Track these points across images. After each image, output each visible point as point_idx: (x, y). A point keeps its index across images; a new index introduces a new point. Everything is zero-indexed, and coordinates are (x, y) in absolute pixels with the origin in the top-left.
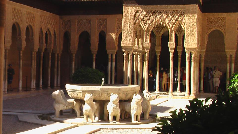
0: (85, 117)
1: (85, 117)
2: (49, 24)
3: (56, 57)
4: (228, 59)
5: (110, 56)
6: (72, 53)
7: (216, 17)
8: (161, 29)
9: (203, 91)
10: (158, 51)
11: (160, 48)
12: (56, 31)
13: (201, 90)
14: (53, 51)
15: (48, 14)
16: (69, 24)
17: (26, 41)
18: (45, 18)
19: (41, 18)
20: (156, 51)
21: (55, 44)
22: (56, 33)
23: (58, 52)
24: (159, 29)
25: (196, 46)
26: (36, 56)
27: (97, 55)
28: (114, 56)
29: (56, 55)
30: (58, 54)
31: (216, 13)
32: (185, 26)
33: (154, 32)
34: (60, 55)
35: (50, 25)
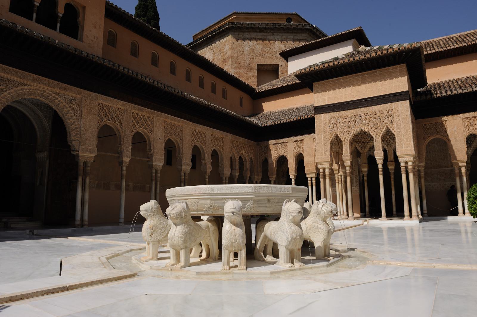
2: (243, 150)
4: (457, 172)
5: (309, 179)
6: (270, 179)
7: (434, 122)
8: (366, 144)
9: (426, 215)
10: (365, 169)
11: (367, 165)
12: (253, 158)
13: (425, 213)
15: (241, 139)
16: (266, 150)
17: (212, 165)
18: (237, 143)
19: (233, 143)
24: (363, 144)
25: (427, 70)
28: (314, 179)
31: (433, 118)
32: (395, 130)
33: (358, 148)
35: (245, 150)
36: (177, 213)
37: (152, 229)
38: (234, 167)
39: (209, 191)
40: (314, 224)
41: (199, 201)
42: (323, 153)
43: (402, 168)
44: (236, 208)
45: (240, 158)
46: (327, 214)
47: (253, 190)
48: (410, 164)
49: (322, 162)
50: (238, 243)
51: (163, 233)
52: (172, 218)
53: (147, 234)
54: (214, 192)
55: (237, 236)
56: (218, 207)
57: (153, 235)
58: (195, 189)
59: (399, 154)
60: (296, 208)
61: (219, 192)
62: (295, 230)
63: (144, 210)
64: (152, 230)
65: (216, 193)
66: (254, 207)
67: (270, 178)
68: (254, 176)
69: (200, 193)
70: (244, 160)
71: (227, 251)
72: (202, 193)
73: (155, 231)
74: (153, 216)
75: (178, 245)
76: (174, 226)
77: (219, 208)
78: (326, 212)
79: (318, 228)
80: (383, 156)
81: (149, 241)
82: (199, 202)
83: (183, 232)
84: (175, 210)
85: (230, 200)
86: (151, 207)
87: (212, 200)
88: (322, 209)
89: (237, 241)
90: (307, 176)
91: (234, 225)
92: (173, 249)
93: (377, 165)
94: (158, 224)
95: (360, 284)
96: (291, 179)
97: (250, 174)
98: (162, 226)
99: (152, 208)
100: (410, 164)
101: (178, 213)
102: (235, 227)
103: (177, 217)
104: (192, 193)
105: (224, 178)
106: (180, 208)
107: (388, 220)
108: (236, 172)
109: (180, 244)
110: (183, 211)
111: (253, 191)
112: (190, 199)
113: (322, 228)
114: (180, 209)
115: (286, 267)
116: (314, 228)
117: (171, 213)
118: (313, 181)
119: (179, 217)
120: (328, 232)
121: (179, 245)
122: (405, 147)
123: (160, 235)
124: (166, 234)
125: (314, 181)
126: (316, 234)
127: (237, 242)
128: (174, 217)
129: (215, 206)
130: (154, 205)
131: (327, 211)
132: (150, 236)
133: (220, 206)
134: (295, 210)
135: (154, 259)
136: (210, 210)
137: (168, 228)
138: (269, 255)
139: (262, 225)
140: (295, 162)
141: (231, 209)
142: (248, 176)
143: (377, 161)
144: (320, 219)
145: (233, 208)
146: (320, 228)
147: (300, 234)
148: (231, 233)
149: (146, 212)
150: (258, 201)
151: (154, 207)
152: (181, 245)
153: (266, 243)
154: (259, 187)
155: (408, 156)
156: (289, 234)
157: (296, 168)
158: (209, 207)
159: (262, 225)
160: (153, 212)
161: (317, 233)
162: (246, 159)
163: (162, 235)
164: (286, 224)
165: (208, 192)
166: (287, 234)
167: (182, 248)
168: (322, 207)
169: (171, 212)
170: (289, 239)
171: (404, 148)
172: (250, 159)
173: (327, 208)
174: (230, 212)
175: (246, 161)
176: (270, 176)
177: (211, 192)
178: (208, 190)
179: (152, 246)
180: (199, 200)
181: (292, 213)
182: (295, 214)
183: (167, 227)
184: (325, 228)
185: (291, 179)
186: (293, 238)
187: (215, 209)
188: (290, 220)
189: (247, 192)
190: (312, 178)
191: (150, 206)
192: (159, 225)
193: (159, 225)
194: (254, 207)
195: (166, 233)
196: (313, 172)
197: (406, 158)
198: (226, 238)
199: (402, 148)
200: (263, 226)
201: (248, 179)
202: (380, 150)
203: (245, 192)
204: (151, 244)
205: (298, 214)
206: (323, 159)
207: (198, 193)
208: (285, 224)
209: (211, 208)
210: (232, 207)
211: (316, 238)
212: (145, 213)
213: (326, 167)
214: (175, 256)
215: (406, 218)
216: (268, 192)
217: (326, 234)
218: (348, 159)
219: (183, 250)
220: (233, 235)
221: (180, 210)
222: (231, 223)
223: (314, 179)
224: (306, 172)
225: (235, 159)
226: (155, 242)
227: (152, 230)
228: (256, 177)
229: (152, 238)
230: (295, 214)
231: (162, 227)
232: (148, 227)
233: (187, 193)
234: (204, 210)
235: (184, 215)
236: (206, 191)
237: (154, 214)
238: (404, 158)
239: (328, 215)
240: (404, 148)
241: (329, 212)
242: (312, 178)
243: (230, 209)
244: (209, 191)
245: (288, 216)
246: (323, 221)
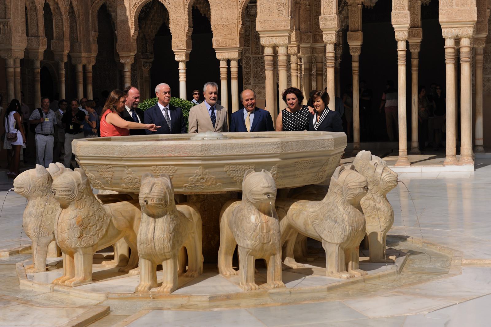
0: (144, 265)
1: (144, 265)
3: (81, 75)
5: (223, 64)
6: (122, 61)
9: (481, 149)
11: (360, 34)
13: (478, 146)
14: (69, 56)
20: (350, 44)
21: (73, 40)
22: (75, 9)
23: (84, 61)
26: (19, 70)
27: (188, 65)
28: (234, 64)
29: (80, 68)
30: (84, 67)
34: (90, 68)
36: (160, 197)
37: (82, 225)
38: (32, 31)
39: (201, 152)
40: (368, 201)
41: (177, 169)
42: (276, 10)
43: (447, 51)
44: (271, 187)
45: (47, 7)
46: (390, 185)
47: (280, 148)
48: (465, 42)
49: (272, 31)
50: (272, 244)
51: (100, 231)
52: (151, 206)
53: (73, 235)
54: (212, 155)
55: (271, 232)
56: (215, 181)
57: (84, 235)
58: (169, 147)
59: (444, 20)
60: (360, 181)
61: (219, 153)
62: (356, 217)
63: (64, 189)
64: (82, 227)
65: (214, 155)
66: (277, 178)
67: (123, 57)
68: (80, 52)
69: (182, 155)
70: (54, 10)
71: (253, 257)
72: (186, 155)
73: (86, 228)
74: (80, 200)
75: (162, 252)
76: (151, 219)
77: (216, 182)
78: (389, 181)
79: (375, 209)
80: (409, 22)
81: (77, 248)
82: (176, 171)
83: (170, 230)
84: (156, 191)
85: (254, 171)
86: (77, 182)
87: (206, 167)
88: (383, 175)
89: (270, 241)
90: (218, 56)
91: (265, 214)
92: (147, 261)
93: (395, 43)
94: (91, 214)
95: (480, 297)
96: (178, 62)
97: (69, 49)
98: (97, 219)
99: (79, 185)
100: (465, 42)
101: (161, 197)
102: (267, 217)
103: (159, 204)
104: (162, 156)
105: (11, 62)
106: (162, 188)
107: (412, 163)
108: (39, 45)
109: (166, 250)
110: (167, 193)
111: (279, 151)
112: (157, 165)
113: (382, 209)
114: (164, 189)
115: (340, 278)
116: (369, 209)
117: (149, 198)
118: (232, 69)
119: (162, 204)
120: (391, 215)
121: (164, 253)
122: (457, 5)
123: (95, 234)
124: (104, 232)
125: (234, 69)
126: (371, 220)
127: (271, 243)
128: (156, 204)
129: (210, 179)
130: (81, 179)
131: (391, 180)
132: (79, 237)
133: (219, 179)
134: (358, 184)
135: (87, 281)
136: (198, 186)
137: (106, 220)
138: (290, 257)
139: (284, 209)
140: (187, 21)
141: (264, 187)
142: (66, 52)
143: (396, 34)
144: (379, 192)
145: (268, 187)
146: (379, 209)
147: (362, 224)
148: (262, 228)
149: (67, 193)
150: (286, 166)
151: (82, 182)
152: (167, 253)
153: (287, 239)
154: (288, 142)
155: (462, 24)
156: (346, 223)
157: (190, 34)
158: (198, 181)
159: (284, 209)
160: (80, 191)
161: (372, 217)
162: (58, 8)
163: (98, 234)
164: (341, 208)
165: (200, 154)
166: (344, 223)
167: (168, 257)
168: (382, 172)
169: (149, 196)
170: (348, 233)
171: (455, 7)
172: (68, 7)
173: (390, 175)
174: (263, 193)
175: (61, 13)
176: (121, 54)
177: (205, 154)
178: (200, 149)
179: (82, 256)
180: (176, 168)
181: (353, 190)
182: (358, 192)
183: (105, 219)
184: (386, 209)
185: (178, 62)
186: (353, 230)
187: (209, 184)
188: (349, 200)
189: (269, 152)
190: (229, 62)
191: (75, 181)
192: (93, 216)
193: (92, 216)
194: (277, 178)
195: (104, 230)
196: (234, 46)
197: (457, 30)
198: (254, 236)
199: (452, 6)
200: (286, 209)
201: (66, 60)
202: (404, 7)
203: (266, 153)
204: (82, 253)
205: (363, 191)
206: (274, 24)
207: (176, 155)
208: (339, 207)
209: (201, 183)
210: (266, 185)
211: (370, 225)
212: (66, 195)
213: (281, 42)
214: (151, 273)
215: (448, 159)
216: (301, 151)
217: (389, 218)
218: (333, 26)
219: (169, 261)
220: (265, 231)
221: (164, 191)
222: (260, 210)
223: (234, 64)
224: (214, 46)
225: (36, 8)
226: (86, 248)
227: (82, 227)
228: (84, 54)
229: (83, 242)
230: (357, 191)
231: (98, 220)
232: (74, 221)
233: (150, 156)
234: (185, 187)
235: (170, 199)
236: (195, 152)
237: (82, 196)
238: (453, 30)
239: (392, 186)
240: (455, 7)
241: (394, 181)
242: (229, 62)
243: (262, 188)
244: (201, 152)
245: (344, 194)
246: (382, 196)
